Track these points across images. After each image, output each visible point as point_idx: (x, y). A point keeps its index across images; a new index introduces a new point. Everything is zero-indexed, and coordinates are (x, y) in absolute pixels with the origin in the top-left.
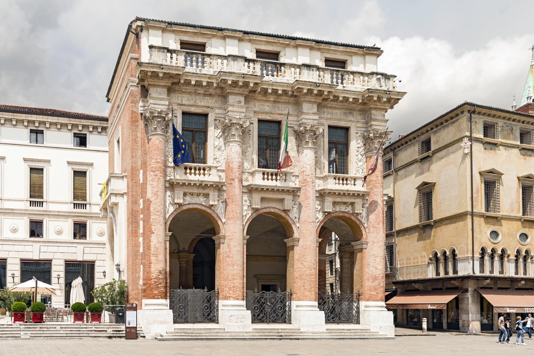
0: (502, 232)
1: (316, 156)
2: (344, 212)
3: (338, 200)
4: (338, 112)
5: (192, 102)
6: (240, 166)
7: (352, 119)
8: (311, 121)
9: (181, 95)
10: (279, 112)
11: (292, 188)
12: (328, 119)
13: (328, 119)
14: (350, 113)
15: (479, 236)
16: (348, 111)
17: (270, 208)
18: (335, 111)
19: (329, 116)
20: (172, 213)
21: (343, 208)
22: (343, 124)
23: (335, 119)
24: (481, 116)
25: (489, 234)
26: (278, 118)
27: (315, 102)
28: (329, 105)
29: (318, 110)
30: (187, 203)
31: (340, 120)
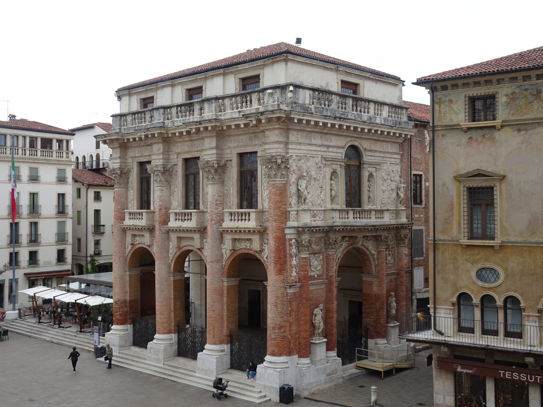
0: (506, 270)
1: (226, 188)
2: (248, 249)
3: (237, 237)
4: (244, 137)
5: (140, 154)
6: (160, 209)
7: (257, 143)
8: (210, 156)
9: (134, 149)
10: (195, 149)
11: (192, 228)
12: (235, 147)
13: (235, 147)
14: (255, 136)
15: (452, 277)
16: (253, 135)
17: (188, 246)
18: (241, 138)
19: (235, 145)
20: (129, 252)
21: (248, 244)
22: (250, 150)
23: (241, 146)
24: (460, 90)
25: (474, 274)
26: (196, 155)
27: (213, 136)
28: (232, 134)
29: (217, 142)
30: (137, 242)
31: (246, 146)
